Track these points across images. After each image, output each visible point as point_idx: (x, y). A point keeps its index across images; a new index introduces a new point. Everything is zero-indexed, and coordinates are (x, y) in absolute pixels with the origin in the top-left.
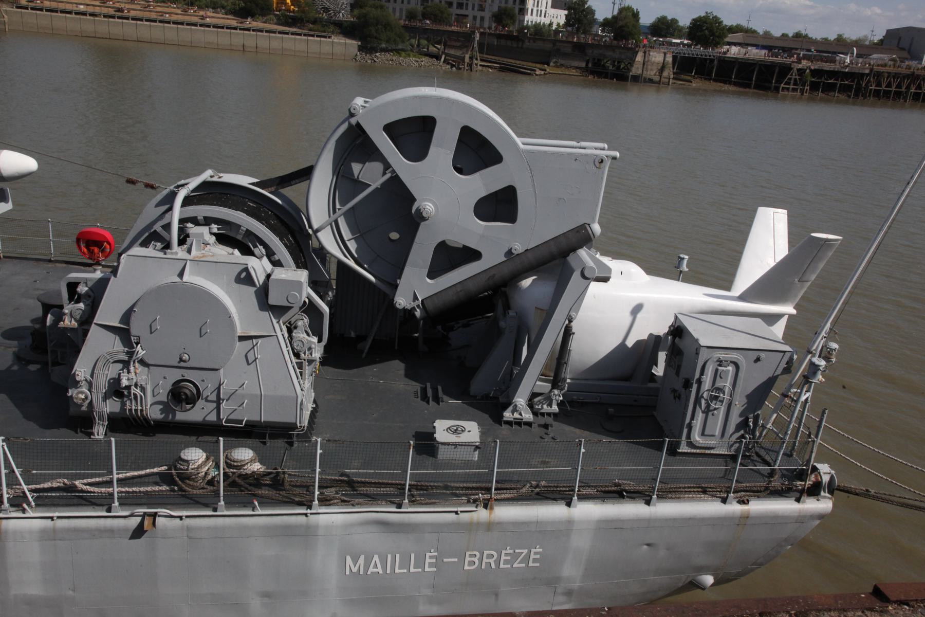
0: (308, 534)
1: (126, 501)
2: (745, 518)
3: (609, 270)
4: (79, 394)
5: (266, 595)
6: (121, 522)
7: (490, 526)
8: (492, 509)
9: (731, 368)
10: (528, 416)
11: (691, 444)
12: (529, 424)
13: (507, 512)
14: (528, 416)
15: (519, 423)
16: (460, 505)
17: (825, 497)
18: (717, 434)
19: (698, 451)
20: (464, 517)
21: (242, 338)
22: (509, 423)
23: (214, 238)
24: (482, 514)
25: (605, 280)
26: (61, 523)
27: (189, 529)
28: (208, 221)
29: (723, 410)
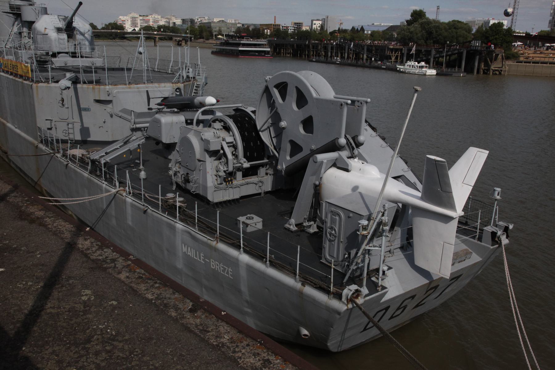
0: (173, 228)
1: (146, 200)
2: (301, 294)
3: (348, 165)
4: (171, 173)
5: (168, 250)
6: (142, 207)
7: (216, 250)
8: (217, 242)
9: (337, 218)
10: (293, 228)
11: (326, 259)
12: (292, 232)
13: (222, 246)
14: (293, 228)
15: (289, 230)
16: (211, 237)
17: (344, 303)
18: (335, 256)
19: (327, 263)
20: (209, 241)
21: (199, 161)
22: (286, 229)
23: (222, 127)
24: (214, 243)
25: (347, 170)
26: (134, 202)
27: (153, 215)
28: (221, 121)
29: (336, 241)
